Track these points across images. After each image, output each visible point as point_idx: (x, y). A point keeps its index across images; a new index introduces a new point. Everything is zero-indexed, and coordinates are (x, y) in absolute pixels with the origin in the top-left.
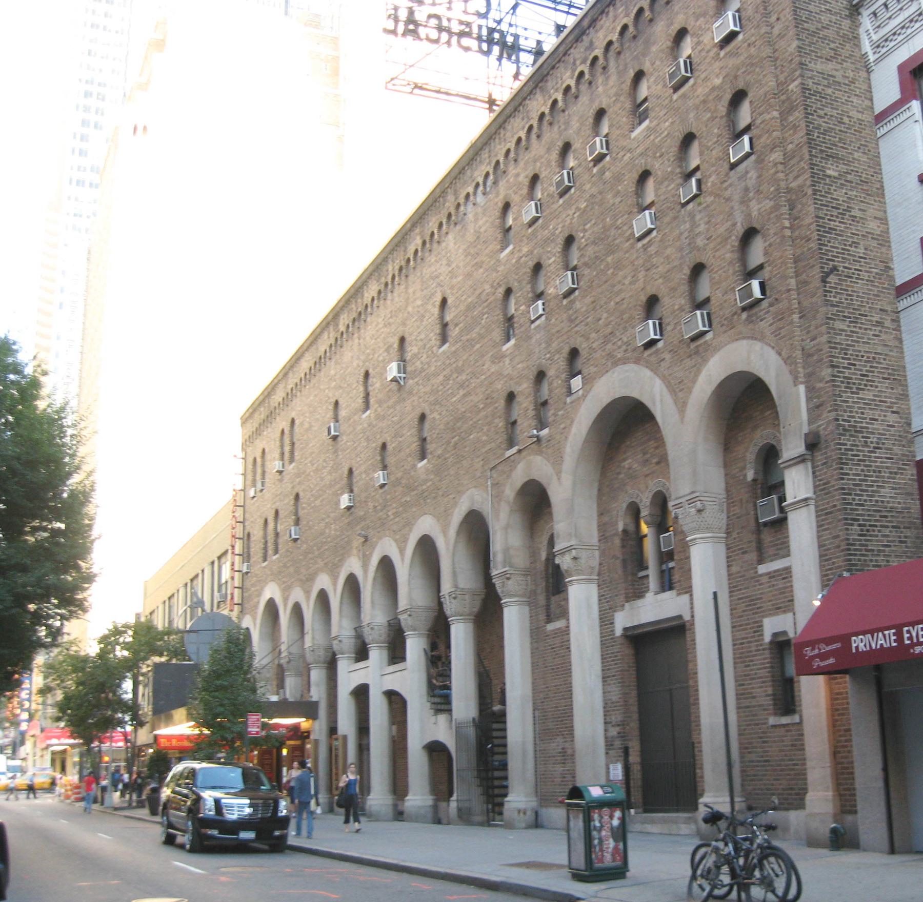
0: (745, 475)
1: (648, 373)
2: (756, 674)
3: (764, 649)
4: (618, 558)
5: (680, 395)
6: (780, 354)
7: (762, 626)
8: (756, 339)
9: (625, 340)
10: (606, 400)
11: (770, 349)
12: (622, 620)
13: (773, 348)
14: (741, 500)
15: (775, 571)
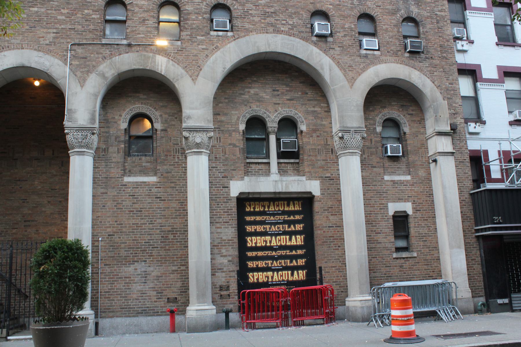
0: (375, 128)
1: (315, 50)
2: (381, 231)
3: (388, 219)
4: (235, 146)
5: (350, 73)
6: (433, 83)
7: (387, 206)
8: (415, 69)
9: (291, 23)
10: (263, 49)
11: (428, 79)
12: (237, 187)
13: (429, 78)
14: (371, 140)
15: (397, 181)
